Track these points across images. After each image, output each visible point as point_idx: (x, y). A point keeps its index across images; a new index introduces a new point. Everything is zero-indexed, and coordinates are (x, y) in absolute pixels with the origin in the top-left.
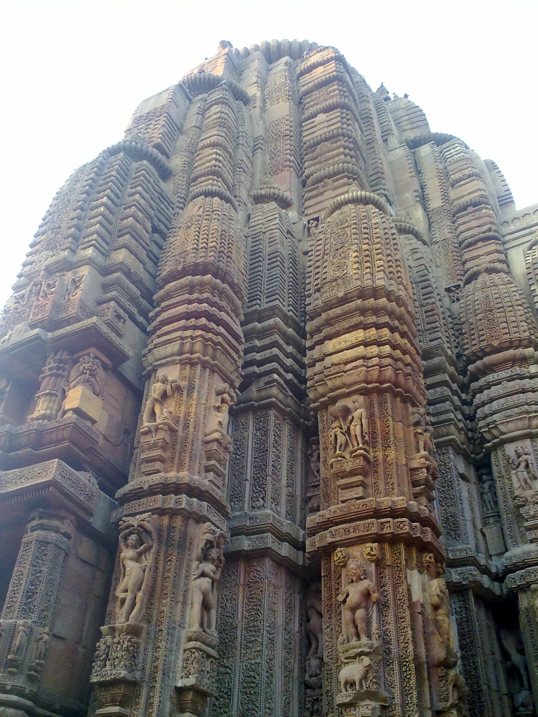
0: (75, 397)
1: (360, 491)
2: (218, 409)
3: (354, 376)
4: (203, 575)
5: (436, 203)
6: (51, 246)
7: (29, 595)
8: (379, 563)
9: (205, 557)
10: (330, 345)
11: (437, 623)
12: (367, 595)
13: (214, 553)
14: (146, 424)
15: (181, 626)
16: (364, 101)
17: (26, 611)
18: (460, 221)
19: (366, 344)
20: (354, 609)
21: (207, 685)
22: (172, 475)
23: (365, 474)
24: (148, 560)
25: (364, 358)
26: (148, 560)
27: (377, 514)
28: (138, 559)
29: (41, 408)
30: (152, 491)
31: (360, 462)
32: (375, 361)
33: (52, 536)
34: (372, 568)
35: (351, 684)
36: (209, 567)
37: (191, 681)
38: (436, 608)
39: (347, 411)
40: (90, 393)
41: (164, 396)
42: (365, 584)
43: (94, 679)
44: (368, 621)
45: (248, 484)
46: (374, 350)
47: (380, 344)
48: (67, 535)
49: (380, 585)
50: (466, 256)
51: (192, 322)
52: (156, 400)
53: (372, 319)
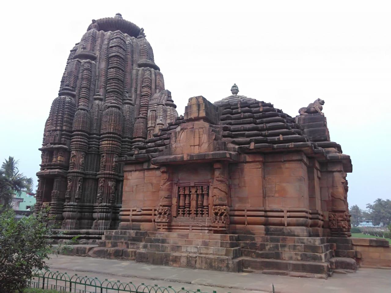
0: (59, 158)
1: (103, 170)
2: (82, 158)
3: (105, 149)
4: (79, 184)
5: (138, 92)
6: (52, 124)
7: (56, 187)
8: (104, 181)
9: (79, 181)
10: (103, 142)
11: (112, 188)
12: (102, 185)
13: (81, 181)
14: (70, 162)
15: (76, 190)
16: (127, 54)
17: (56, 190)
18: (142, 99)
19: (107, 144)
20: (100, 187)
21: (79, 197)
22: (74, 170)
23: (104, 167)
24: (71, 183)
25: (107, 147)
26: (71, 183)
27: (105, 174)
28: (70, 182)
29: (54, 160)
30: (72, 173)
31: (103, 166)
32: (108, 148)
33: (58, 180)
34: (103, 182)
35: (98, 196)
36: (80, 183)
37: (77, 197)
38: (112, 186)
39: (103, 156)
40: (61, 157)
41: (73, 156)
42: (102, 184)
43: (65, 197)
44: (102, 189)
45: (89, 166)
46: (108, 145)
47: (110, 144)
48: (61, 179)
49: (104, 184)
50: (141, 110)
51: (77, 143)
52: (72, 158)
53: (109, 139)
